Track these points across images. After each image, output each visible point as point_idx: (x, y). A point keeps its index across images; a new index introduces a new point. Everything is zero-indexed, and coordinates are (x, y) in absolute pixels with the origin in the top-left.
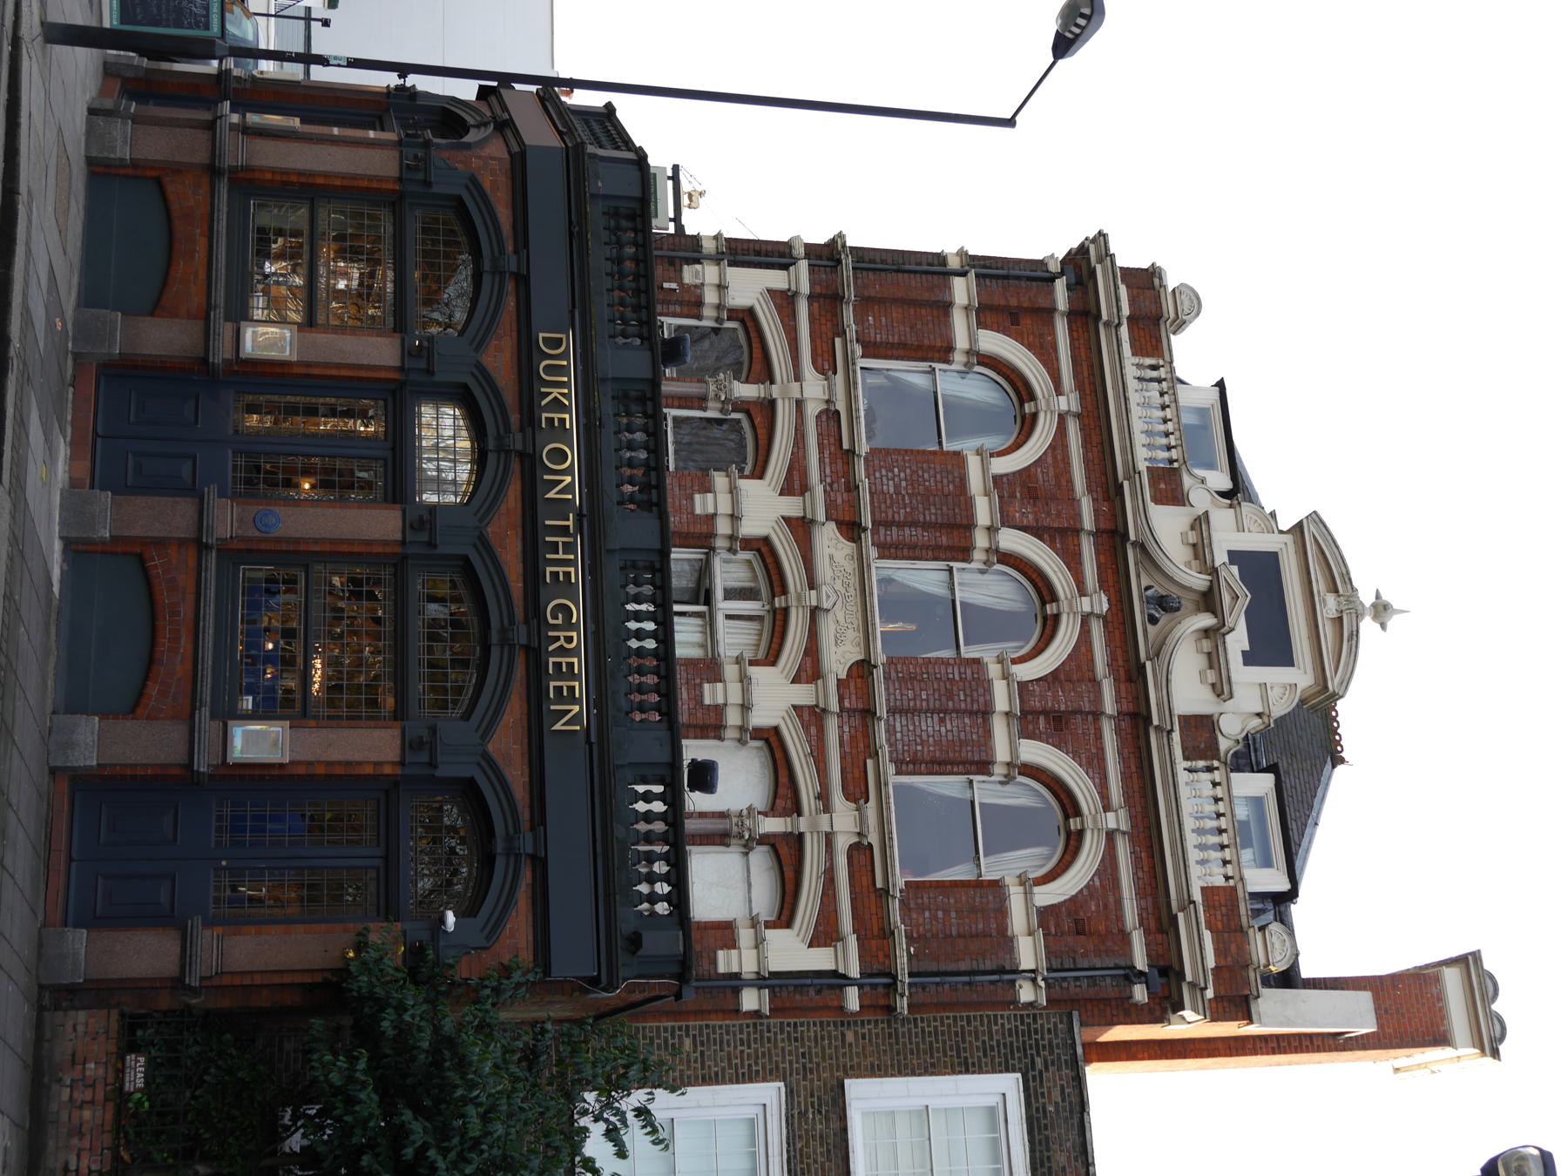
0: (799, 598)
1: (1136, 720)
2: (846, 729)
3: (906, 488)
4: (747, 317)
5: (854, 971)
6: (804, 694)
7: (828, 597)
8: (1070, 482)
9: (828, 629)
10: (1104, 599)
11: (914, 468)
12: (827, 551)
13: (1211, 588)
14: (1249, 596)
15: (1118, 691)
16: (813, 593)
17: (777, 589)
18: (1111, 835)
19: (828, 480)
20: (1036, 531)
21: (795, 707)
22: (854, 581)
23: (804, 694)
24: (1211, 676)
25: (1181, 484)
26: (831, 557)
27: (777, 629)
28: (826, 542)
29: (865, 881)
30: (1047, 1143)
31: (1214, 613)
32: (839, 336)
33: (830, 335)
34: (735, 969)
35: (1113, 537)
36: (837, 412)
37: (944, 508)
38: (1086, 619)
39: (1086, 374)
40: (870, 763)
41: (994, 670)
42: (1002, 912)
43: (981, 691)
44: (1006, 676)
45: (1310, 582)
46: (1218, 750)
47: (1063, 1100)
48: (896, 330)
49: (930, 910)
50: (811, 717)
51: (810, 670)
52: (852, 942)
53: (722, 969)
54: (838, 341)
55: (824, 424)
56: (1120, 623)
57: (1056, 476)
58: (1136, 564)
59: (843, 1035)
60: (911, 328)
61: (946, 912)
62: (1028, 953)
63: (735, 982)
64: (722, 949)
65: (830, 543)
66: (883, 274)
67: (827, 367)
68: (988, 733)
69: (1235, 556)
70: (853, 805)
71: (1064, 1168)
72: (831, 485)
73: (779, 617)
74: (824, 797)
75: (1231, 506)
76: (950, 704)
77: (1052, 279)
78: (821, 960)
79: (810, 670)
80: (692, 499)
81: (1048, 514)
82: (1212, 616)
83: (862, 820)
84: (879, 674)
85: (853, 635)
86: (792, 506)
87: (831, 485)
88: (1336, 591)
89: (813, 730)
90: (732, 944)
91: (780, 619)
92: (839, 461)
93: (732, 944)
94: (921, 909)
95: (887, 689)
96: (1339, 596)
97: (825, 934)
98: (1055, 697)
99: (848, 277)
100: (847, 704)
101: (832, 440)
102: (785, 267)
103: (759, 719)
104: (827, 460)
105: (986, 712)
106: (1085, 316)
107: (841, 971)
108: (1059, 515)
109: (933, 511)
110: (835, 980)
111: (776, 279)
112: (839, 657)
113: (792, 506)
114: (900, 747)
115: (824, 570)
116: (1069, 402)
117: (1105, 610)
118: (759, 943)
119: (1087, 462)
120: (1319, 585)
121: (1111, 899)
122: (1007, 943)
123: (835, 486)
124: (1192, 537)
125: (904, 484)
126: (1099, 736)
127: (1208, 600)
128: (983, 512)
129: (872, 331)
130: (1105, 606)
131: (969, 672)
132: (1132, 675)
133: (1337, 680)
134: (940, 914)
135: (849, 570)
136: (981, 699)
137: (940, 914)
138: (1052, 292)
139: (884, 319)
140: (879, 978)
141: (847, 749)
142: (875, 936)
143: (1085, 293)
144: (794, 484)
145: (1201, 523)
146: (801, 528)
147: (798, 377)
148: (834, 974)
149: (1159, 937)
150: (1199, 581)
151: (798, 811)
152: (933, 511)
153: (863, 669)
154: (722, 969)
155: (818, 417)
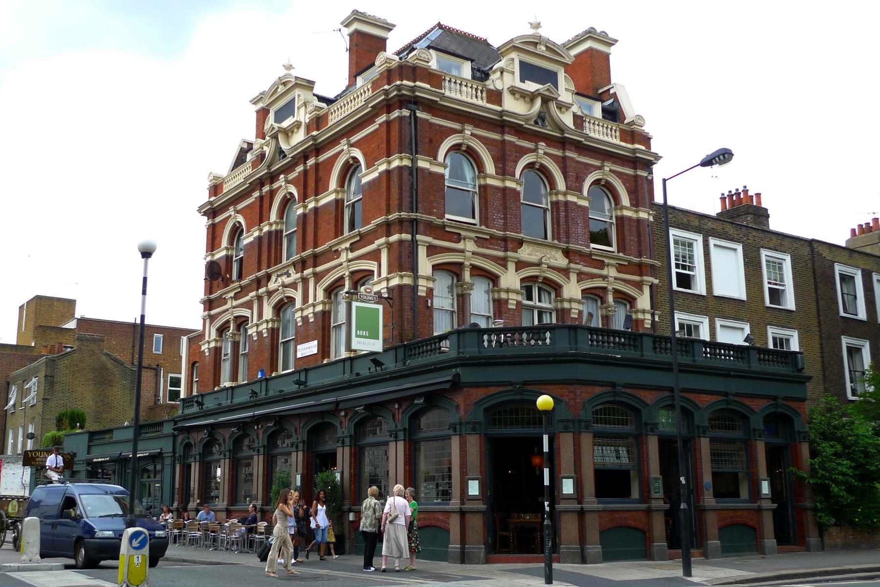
0: (544, 272)
1: (580, 147)
2: (582, 263)
3: (501, 214)
4: (436, 268)
5: (651, 279)
6: (573, 277)
7: (546, 260)
8: (494, 140)
9: (553, 262)
10: (541, 143)
11: (493, 209)
12: (526, 256)
13: (542, 98)
14: (549, 84)
15: (570, 150)
16: (543, 265)
17: (534, 279)
18: (611, 171)
19: (499, 248)
20: (516, 162)
21: (578, 282)
22: (536, 248)
23: (573, 277)
24: (563, 110)
25: (492, 90)
26: (528, 254)
27: (548, 283)
28: (523, 255)
29: (624, 268)
30: (683, 224)
31: (550, 100)
32: (445, 228)
33: (442, 232)
34: (650, 322)
35: (519, 131)
36: (476, 237)
37: (511, 201)
38: (545, 153)
39: (451, 116)
40: (593, 257)
41: (561, 198)
42: (630, 219)
43: (571, 206)
44: (565, 194)
45: (543, 56)
46: (581, 116)
47: (672, 214)
48: (439, 200)
49: (631, 247)
50: (581, 277)
51: (565, 272)
52: (645, 278)
53: (649, 327)
54: (447, 229)
55: (479, 244)
56: (549, 140)
57: (493, 145)
58: (530, 125)
59: (660, 287)
60: (437, 192)
61: (631, 240)
62: (643, 215)
63: (653, 321)
64: (644, 325)
65: (526, 253)
66: (419, 199)
67: (456, 237)
68: (581, 207)
69: (522, 80)
70: (606, 268)
71: (688, 220)
72: (501, 248)
73: (546, 282)
74: (604, 277)
75: (502, 73)
76: (576, 220)
77: (416, 118)
78: (647, 290)
79: (565, 272)
80: (510, 309)
81: (510, 155)
82: (552, 102)
83: (612, 265)
84: (572, 246)
85: (554, 252)
86: (511, 266)
87: (501, 248)
88: (537, 43)
89: (582, 276)
90: (643, 321)
91: (547, 281)
92: (493, 241)
93: (643, 321)
94: (631, 249)
95: (573, 244)
96: (540, 43)
97: (639, 286)
98: (572, 176)
99: (426, 218)
100: (578, 261)
101: (484, 242)
102: (417, 245)
103: (579, 296)
104: (492, 247)
105: (575, 203)
106: (431, 107)
107: (650, 284)
108: (511, 151)
109: (512, 206)
110: (651, 286)
111: (422, 252)
112: (561, 261)
113: (511, 266)
114: (586, 243)
115: (534, 258)
116: (469, 130)
117: (545, 145)
118: (644, 312)
119: (488, 130)
120: (531, 48)
121: (625, 177)
122: (639, 221)
123: (501, 245)
124: (517, 96)
125: (499, 215)
126: (578, 162)
127: (546, 101)
128: (510, 184)
129: (440, 211)
130: (543, 144)
131: (562, 208)
132: (563, 143)
133: (568, 59)
134: (632, 243)
135: (531, 247)
136: (574, 207)
137: (632, 243)
138: (421, 119)
139: (434, 204)
140: (653, 270)
141: (588, 265)
142: (640, 269)
143: (422, 103)
144: (503, 262)
145: (513, 91)
146: (521, 265)
147: (462, 251)
148: (651, 287)
149: (638, 164)
150: (538, 102)
151: (605, 289)
152: (512, 206)
153: (567, 253)
154: (649, 327)
155: (479, 246)
